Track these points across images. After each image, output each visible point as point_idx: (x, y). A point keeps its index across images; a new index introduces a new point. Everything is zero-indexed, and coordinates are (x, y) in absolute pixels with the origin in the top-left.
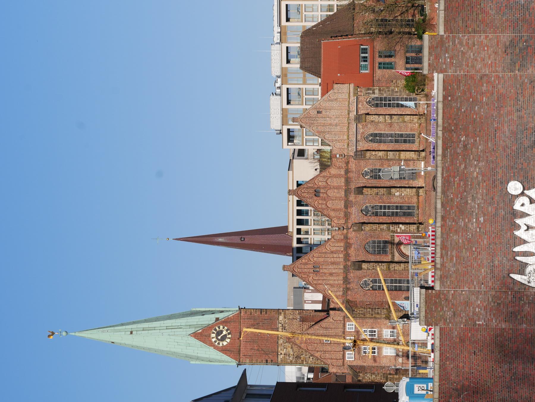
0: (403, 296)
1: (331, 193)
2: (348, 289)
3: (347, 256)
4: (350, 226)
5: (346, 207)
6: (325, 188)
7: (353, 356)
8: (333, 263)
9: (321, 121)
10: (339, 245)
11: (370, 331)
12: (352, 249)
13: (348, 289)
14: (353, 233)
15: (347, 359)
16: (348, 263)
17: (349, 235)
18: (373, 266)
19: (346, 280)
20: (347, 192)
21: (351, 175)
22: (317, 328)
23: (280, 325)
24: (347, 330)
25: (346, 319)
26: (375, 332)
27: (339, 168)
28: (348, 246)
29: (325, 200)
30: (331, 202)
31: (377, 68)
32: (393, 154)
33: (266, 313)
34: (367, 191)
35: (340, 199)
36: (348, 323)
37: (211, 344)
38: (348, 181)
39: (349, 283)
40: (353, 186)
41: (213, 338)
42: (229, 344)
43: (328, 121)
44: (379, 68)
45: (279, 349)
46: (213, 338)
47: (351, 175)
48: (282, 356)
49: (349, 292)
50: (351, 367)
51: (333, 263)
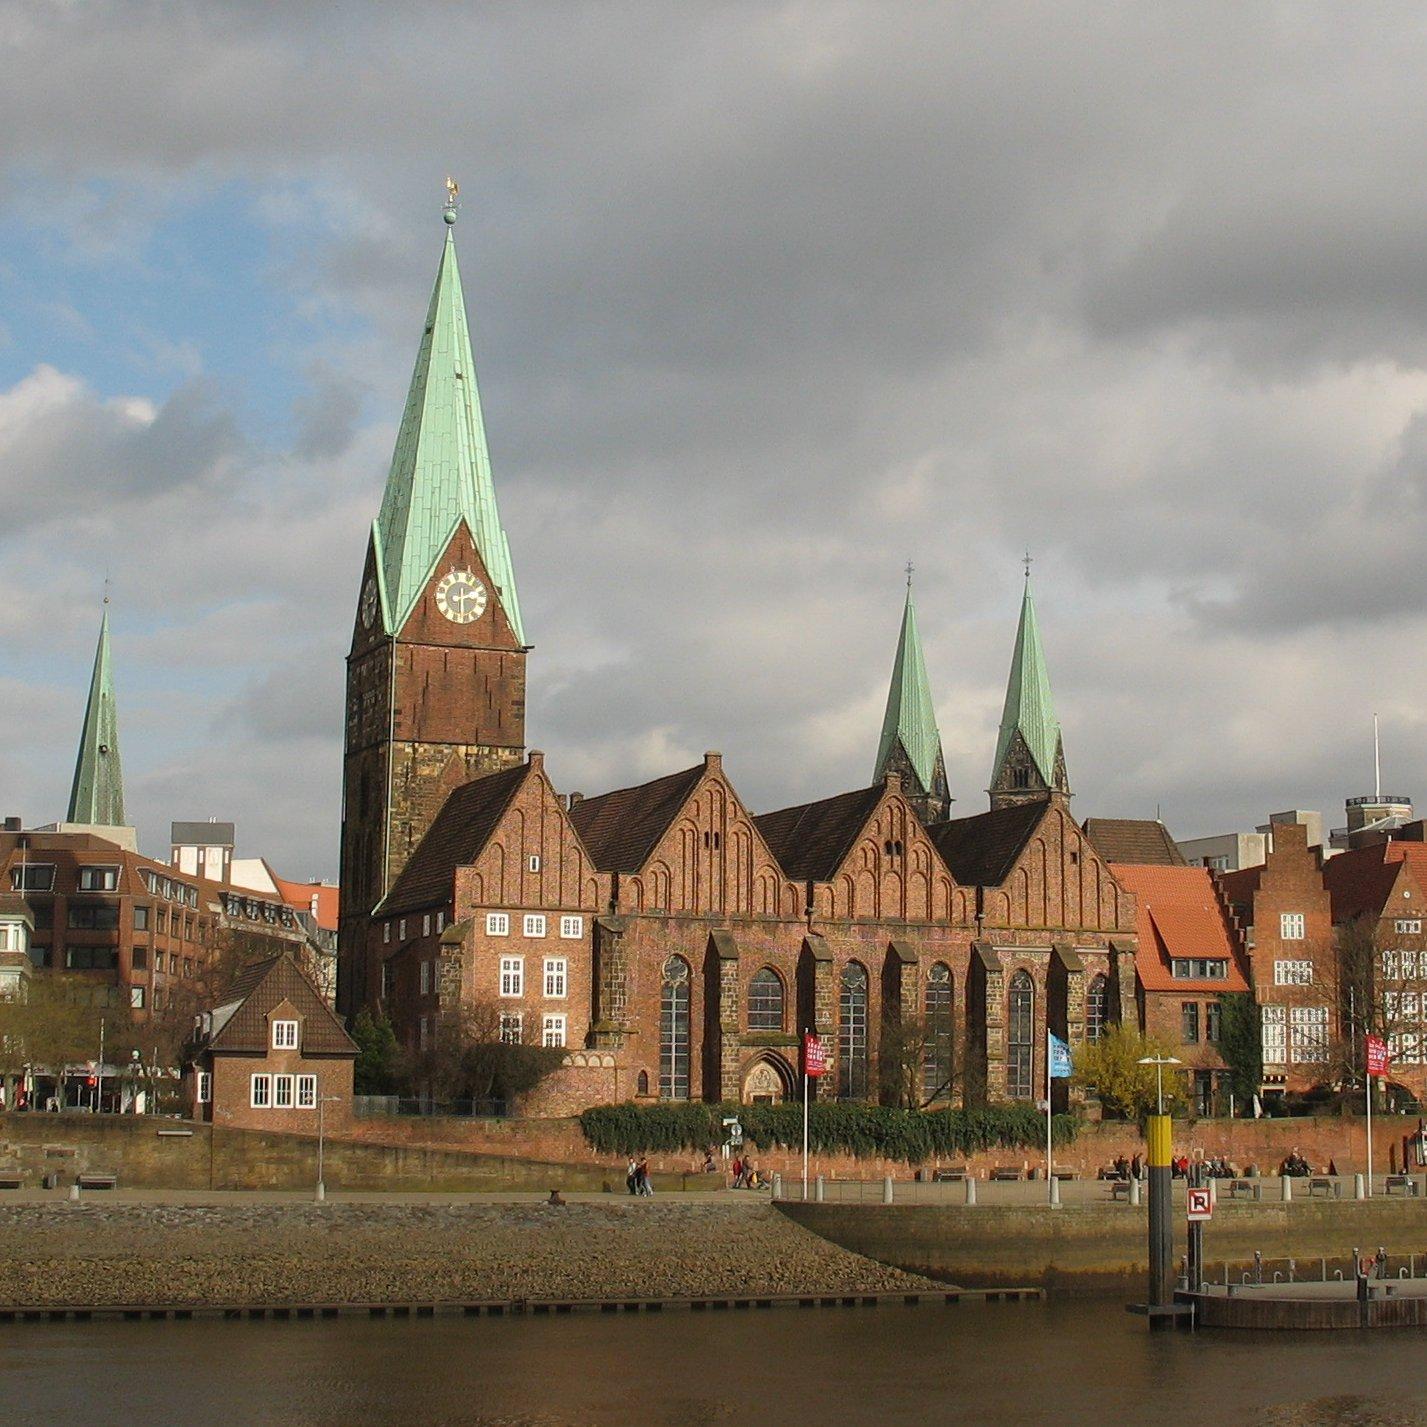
0: (648, 1070)
1: (890, 883)
2: (665, 921)
3: (744, 922)
4: (818, 929)
5: (862, 923)
6: (904, 864)
7: (497, 933)
8: (723, 883)
9: (1053, 860)
10: (770, 900)
11: (559, 978)
12: (762, 936)
13: (665, 921)
14: (801, 939)
15: (489, 916)
16: (727, 923)
17: (795, 928)
18: (729, 990)
19: (684, 920)
20: (900, 924)
21: (937, 934)
22: (569, 839)
23: (486, 751)
24: (563, 919)
25: (590, 915)
26: (559, 992)
27: (949, 905)
28: (770, 925)
29: (877, 866)
30: (872, 881)
31: (1185, 999)
32: (997, 1042)
33: (517, 716)
34: (909, 975)
35: (877, 905)
36: (580, 919)
37: (440, 573)
38: (924, 926)
39: (680, 926)
40: (912, 938)
41: (457, 578)
42: (442, 617)
43: (1054, 881)
44: (1184, 1005)
45: (426, 746)
46: (457, 578)
47: (937, 934)
48: (409, 750)
49: (657, 925)
50: (468, 925)
51: (723, 883)
